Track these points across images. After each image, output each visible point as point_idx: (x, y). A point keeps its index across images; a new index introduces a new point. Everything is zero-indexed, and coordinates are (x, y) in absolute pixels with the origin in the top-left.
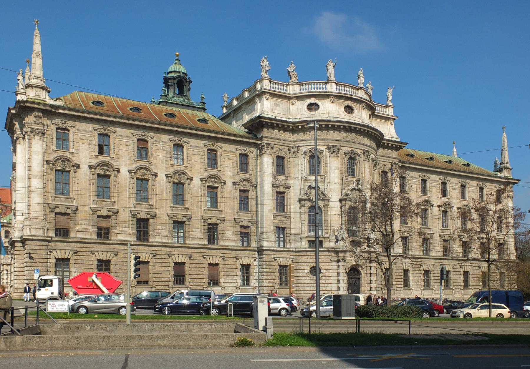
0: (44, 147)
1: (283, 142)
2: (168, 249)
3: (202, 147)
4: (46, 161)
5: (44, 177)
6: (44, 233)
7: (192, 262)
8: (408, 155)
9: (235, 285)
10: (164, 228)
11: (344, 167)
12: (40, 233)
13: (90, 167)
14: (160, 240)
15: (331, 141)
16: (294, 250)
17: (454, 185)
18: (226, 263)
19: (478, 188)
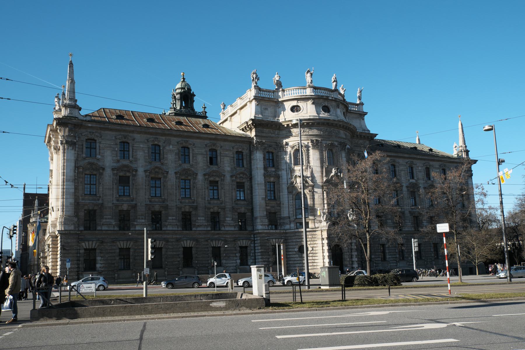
0: (76, 155)
4: (77, 167)
9: (235, 265)
10: (174, 218)
13: (113, 169)
14: (171, 229)
15: (313, 137)
16: (285, 231)
17: (420, 168)
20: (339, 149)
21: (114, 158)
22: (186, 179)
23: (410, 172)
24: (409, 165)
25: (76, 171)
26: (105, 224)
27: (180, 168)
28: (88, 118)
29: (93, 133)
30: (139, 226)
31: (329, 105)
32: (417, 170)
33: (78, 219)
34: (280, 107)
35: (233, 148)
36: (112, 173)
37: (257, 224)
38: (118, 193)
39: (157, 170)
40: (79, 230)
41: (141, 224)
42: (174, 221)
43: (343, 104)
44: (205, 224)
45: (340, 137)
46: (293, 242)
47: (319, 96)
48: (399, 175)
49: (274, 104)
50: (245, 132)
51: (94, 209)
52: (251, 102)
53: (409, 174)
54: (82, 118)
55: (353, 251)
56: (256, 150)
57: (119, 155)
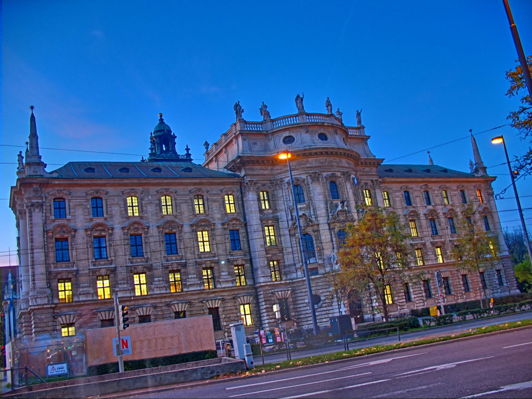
0: (44, 218)
1: (265, 177)
2: (167, 300)
3: (189, 195)
5: (45, 247)
6: (49, 301)
7: (192, 309)
8: (387, 171)
10: (161, 279)
11: (327, 192)
12: (46, 301)
13: (86, 230)
14: (158, 292)
15: (310, 169)
16: (291, 281)
17: (436, 192)
18: (227, 305)
19: (459, 191)
20: (343, 180)
21: (87, 217)
22: (171, 232)
23: (426, 198)
24: (424, 190)
25: (46, 236)
26: (82, 294)
27: (162, 221)
28: (55, 175)
29: (61, 191)
30: (121, 292)
31: (326, 132)
32: (434, 195)
33: (52, 290)
34: (270, 140)
35: (221, 191)
36: (85, 234)
37: (258, 276)
38: (94, 256)
39: (136, 226)
40: (53, 304)
41: (124, 290)
42: (161, 282)
43: (342, 129)
44: (197, 282)
45: (342, 167)
46: (302, 292)
47: (312, 123)
48: (414, 202)
49: (264, 137)
50: (233, 171)
51: (69, 277)
52: (236, 137)
53: (425, 200)
54: (49, 176)
55: (372, 294)
56: (248, 191)
57: (91, 213)
